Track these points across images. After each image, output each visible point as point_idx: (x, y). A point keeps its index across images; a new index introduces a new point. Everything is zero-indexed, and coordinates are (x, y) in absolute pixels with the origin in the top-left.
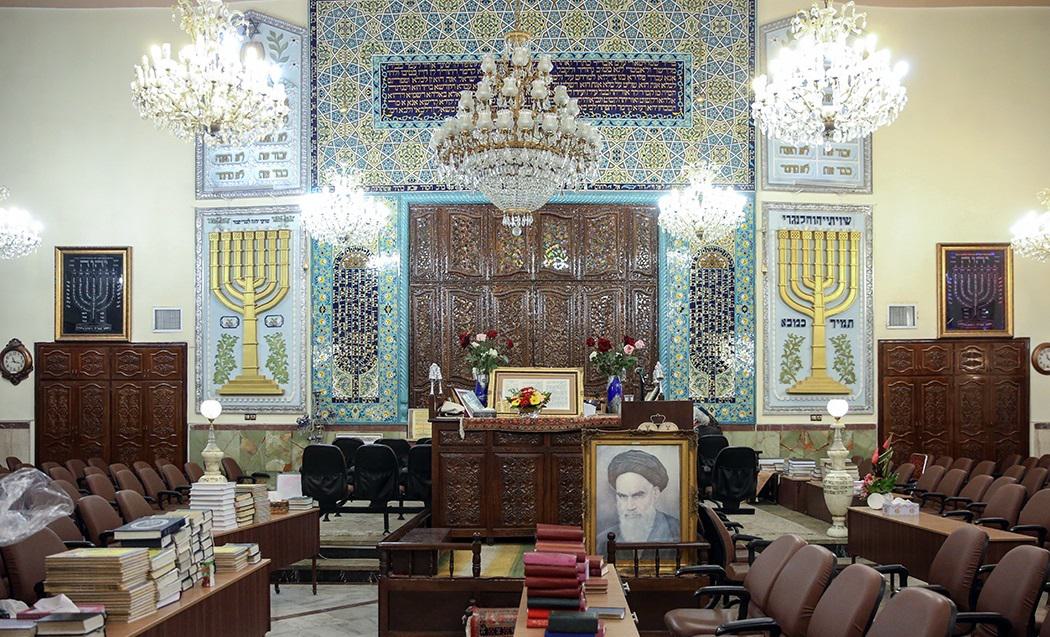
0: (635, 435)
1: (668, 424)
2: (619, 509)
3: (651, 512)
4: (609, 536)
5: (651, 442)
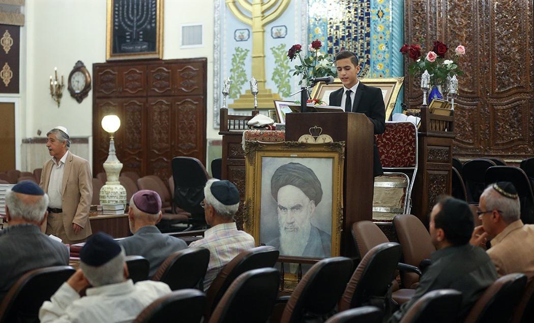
0: (295, 147)
1: (324, 136)
5: (307, 154)
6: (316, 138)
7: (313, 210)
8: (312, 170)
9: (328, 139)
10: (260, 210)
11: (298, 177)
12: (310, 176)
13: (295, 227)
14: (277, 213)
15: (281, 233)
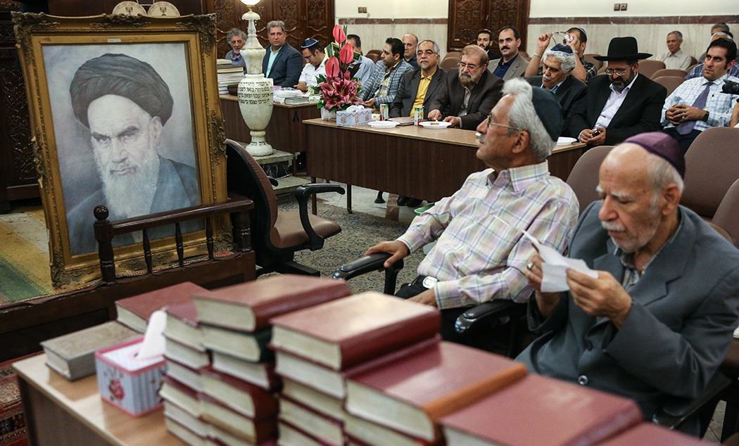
2: (98, 163)
3: (151, 160)
4: (96, 214)
5: (140, 37)
6: (147, 9)
7: (159, 133)
8: (151, 67)
9: (172, 12)
10: (55, 148)
11: (124, 79)
12: (147, 75)
13: (130, 166)
14: (91, 148)
15: (104, 181)
